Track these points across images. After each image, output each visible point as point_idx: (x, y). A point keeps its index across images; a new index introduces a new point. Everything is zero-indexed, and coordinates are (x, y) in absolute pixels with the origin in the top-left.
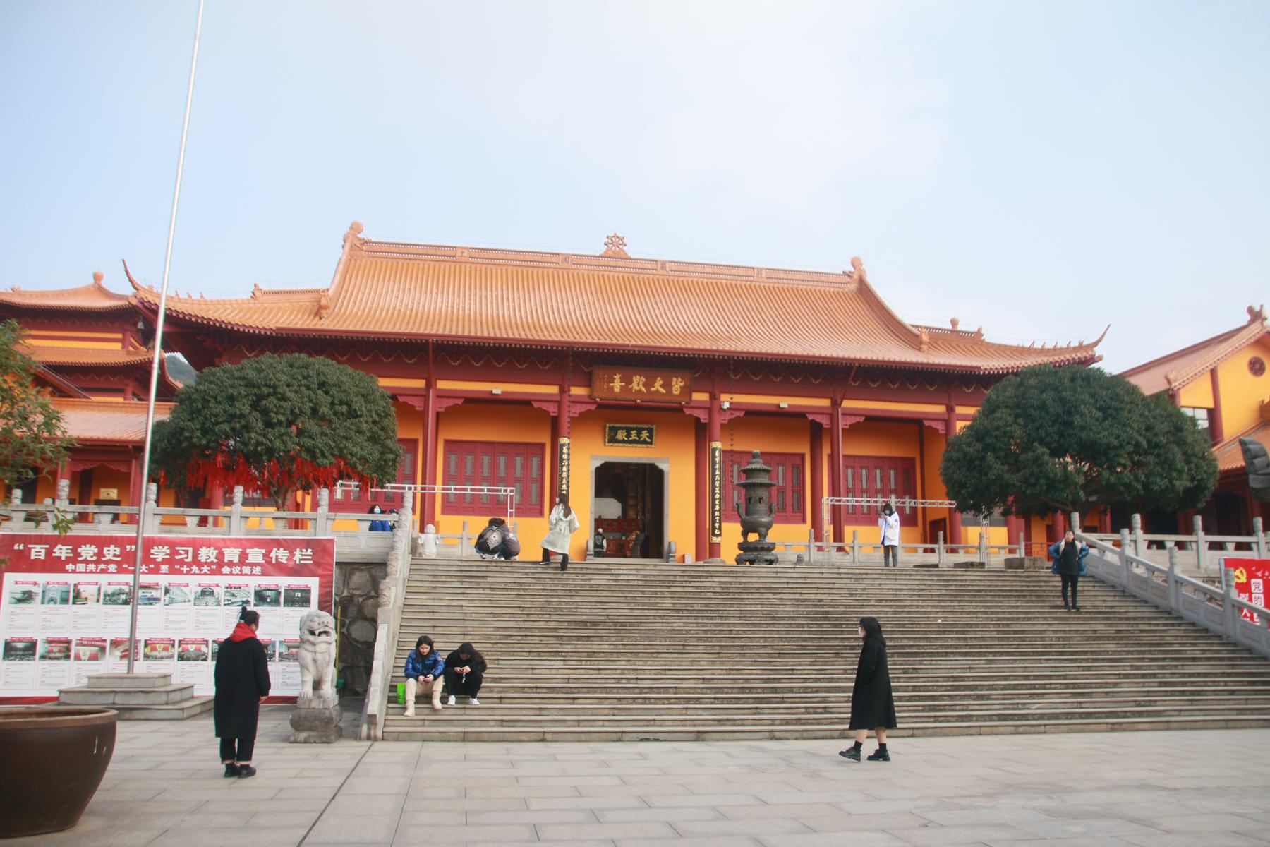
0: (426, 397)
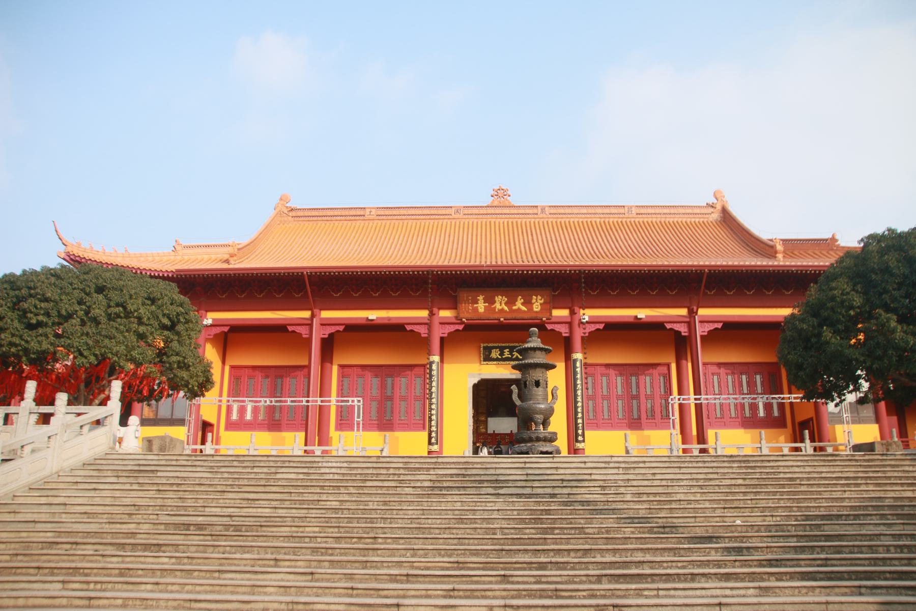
0: (311, 325)
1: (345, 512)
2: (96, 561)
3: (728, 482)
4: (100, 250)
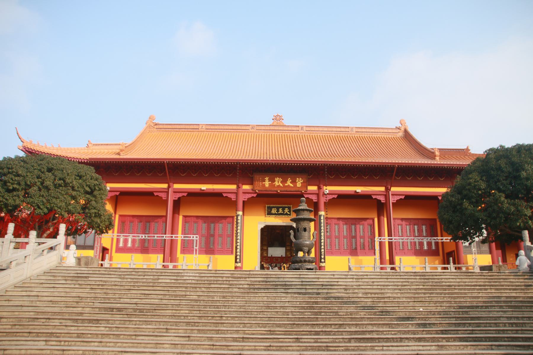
1: (202, 302)
2: (62, 329)
3: (415, 287)
4: (44, 145)
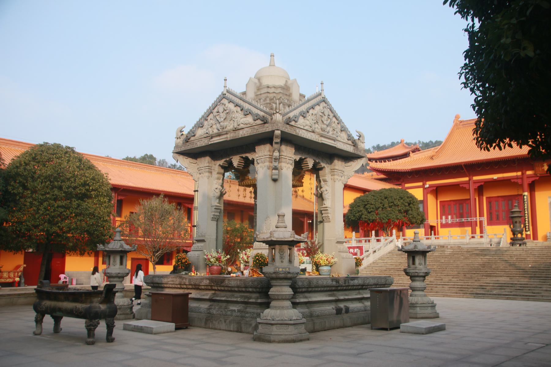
0: (469, 183)
